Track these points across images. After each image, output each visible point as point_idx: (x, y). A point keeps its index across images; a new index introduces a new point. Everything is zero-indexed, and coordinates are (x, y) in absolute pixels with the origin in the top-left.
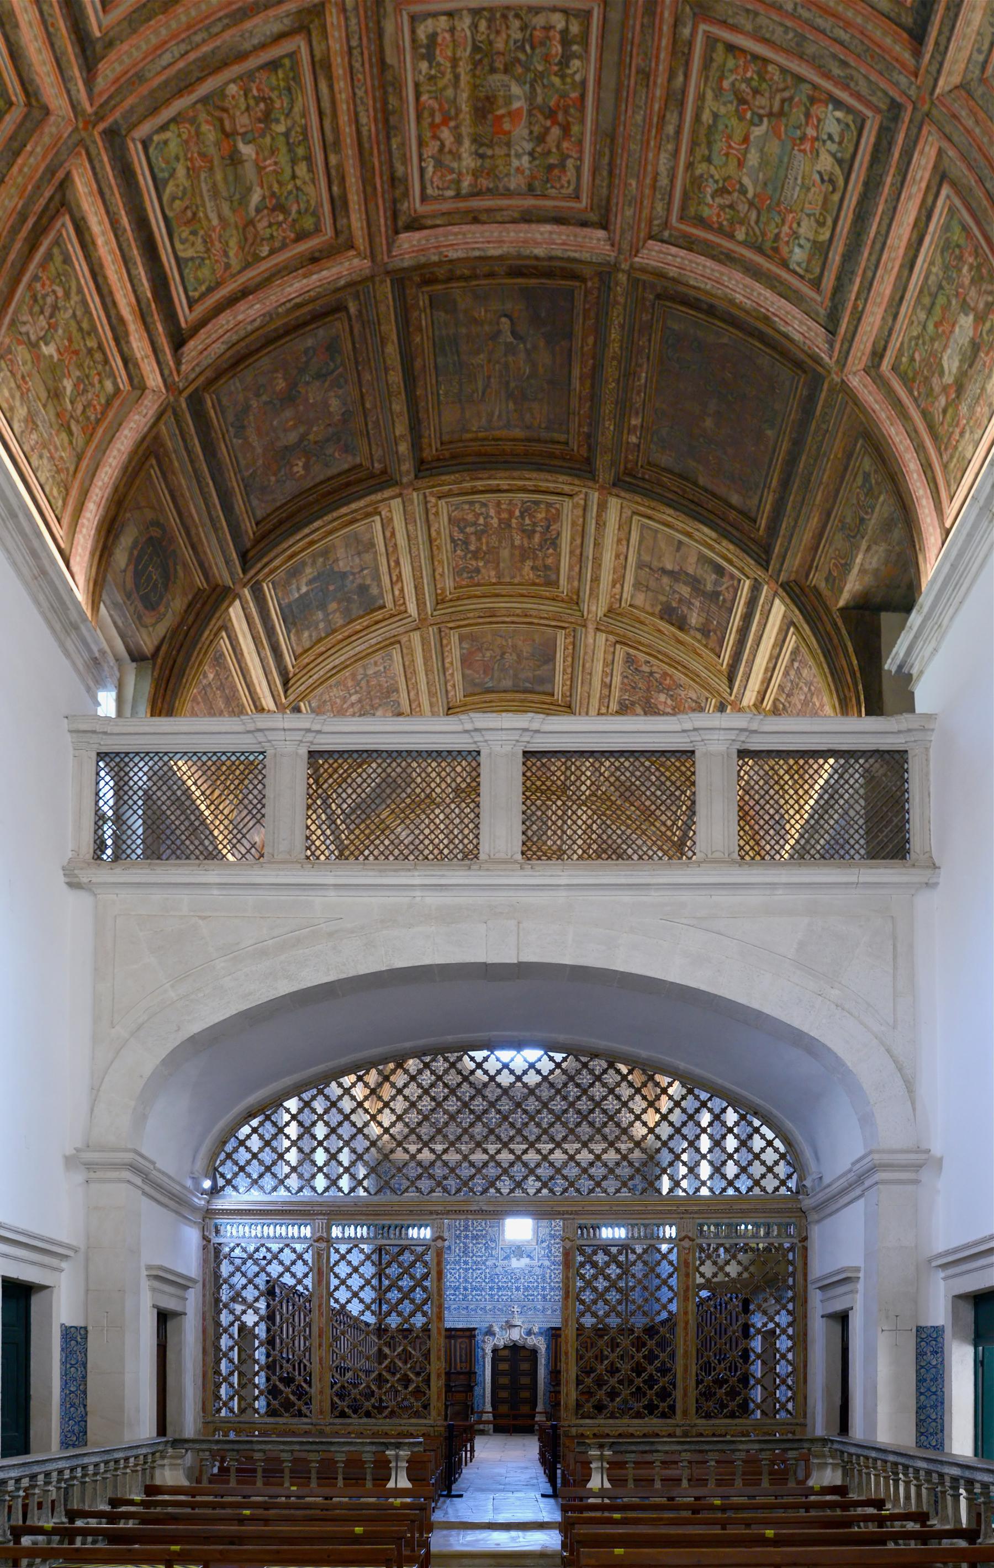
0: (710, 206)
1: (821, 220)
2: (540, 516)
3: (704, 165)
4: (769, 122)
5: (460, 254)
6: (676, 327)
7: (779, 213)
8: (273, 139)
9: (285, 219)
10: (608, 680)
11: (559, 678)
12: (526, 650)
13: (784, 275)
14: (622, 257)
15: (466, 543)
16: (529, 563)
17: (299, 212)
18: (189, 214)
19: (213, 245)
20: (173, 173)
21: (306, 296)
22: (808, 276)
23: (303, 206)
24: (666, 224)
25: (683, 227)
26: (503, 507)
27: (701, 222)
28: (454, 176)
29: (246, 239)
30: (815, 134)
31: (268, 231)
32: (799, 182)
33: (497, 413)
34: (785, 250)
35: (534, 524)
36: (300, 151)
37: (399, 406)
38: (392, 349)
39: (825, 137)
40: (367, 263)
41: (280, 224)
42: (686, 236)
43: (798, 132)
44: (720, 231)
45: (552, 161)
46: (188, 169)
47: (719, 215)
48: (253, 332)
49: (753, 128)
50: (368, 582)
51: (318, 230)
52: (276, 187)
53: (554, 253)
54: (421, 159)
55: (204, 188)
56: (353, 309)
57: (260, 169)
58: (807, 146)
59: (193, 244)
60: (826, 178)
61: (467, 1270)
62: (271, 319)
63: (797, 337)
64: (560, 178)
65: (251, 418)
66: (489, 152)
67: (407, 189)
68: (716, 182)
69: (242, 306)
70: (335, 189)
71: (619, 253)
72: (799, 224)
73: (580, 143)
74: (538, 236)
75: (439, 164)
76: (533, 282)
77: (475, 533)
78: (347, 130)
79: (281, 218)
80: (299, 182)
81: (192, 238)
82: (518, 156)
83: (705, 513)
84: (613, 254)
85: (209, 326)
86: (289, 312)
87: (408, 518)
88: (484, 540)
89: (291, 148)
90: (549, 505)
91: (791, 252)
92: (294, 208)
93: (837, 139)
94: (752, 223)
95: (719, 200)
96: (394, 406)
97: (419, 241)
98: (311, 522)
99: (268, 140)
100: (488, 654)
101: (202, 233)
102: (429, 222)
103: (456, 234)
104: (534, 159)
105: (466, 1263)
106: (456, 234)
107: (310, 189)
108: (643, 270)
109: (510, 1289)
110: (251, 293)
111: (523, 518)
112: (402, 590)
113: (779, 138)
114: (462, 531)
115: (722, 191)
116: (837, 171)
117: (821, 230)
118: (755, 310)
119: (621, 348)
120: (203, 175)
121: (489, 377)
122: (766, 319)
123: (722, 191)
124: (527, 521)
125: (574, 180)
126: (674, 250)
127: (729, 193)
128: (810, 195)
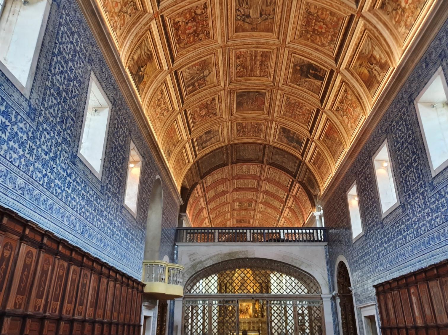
10: (220, 104)
11: (235, 99)
12: (245, 105)
16: (244, 126)
50: (282, 133)
90: (240, 136)
100: (256, 104)
112: (275, 126)
114: (259, 132)
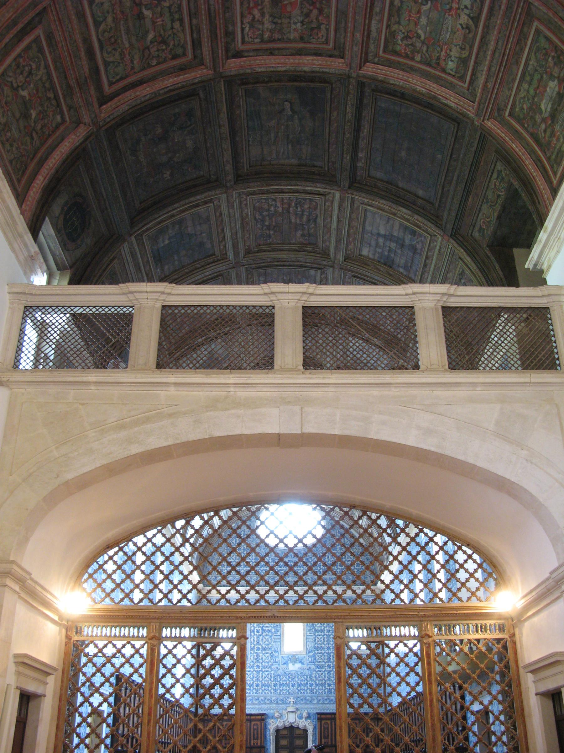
0: (400, 45)
1: (463, 47)
2: (306, 206)
3: (396, 26)
4: (432, 2)
5: (263, 70)
6: (383, 105)
7: (439, 46)
8: (162, 9)
9: (166, 49)
13: (443, 75)
14: (352, 71)
15: (263, 220)
17: (174, 45)
18: (113, 40)
19: (125, 57)
20: (105, 19)
21: (176, 86)
22: (457, 75)
23: (177, 43)
24: (376, 55)
25: (385, 56)
26: (285, 201)
27: (396, 53)
28: (260, 32)
29: (144, 56)
30: (457, 6)
31: (157, 53)
32: (450, 30)
33: (282, 150)
34: (443, 63)
35: (303, 211)
36: (177, 16)
37: (227, 145)
38: (224, 116)
39: (463, 7)
40: (211, 72)
41: (163, 50)
42: (389, 60)
43: (448, 6)
44: (406, 57)
45: (313, 26)
46: (114, 18)
47: (405, 50)
48: (145, 101)
49: (422, 6)
51: (184, 54)
52: (162, 32)
53: (314, 70)
54: (242, 23)
55: (122, 29)
56: (202, 95)
57: (154, 23)
58: (453, 12)
59: (114, 55)
60: (464, 26)
61: (258, 672)
62: (156, 96)
63: (453, 105)
64: (317, 34)
65: (141, 146)
66: (279, 21)
67: (234, 38)
68: (404, 33)
69: (139, 88)
70: (195, 35)
71: (350, 68)
72: (450, 50)
73: (328, 17)
74: (305, 61)
75: (252, 26)
76: (303, 84)
77: (269, 215)
78: (203, 7)
79: (164, 47)
80: (175, 31)
81: (114, 52)
82: (295, 23)
83: (403, 201)
84: (348, 69)
85: (120, 97)
86: (166, 93)
87: (230, 206)
88: (274, 220)
89: (171, 13)
91: (447, 64)
92: (172, 43)
93: (469, 7)
94: (424, 52)
95: (404, 42)
96: (223, 145)
97: (240, 63)
98: (173, 204)
99: (159, 9)
101: (119, 50)
102: (246, 54)
103: (260, 60)
104: (303, 25)
105: (258, 667)
106: (260, 60)
107: (181, 35)
108: (364, 77)
109: (288, 685)
110: (145, 83)
111: (297, 208)
113: (437, 10)
115: (407, 37)
116: (471, 23)
117: (463, 52)
118: (428, 93)
119: (352, 116)
120: (122, 22)
121: (278, 132)
122: (435, 98)
123: (407, 37)
124: (299, 209)
125: (325, 35)
126: (381, 67)
127: (411, 38)
128: (456, 36)
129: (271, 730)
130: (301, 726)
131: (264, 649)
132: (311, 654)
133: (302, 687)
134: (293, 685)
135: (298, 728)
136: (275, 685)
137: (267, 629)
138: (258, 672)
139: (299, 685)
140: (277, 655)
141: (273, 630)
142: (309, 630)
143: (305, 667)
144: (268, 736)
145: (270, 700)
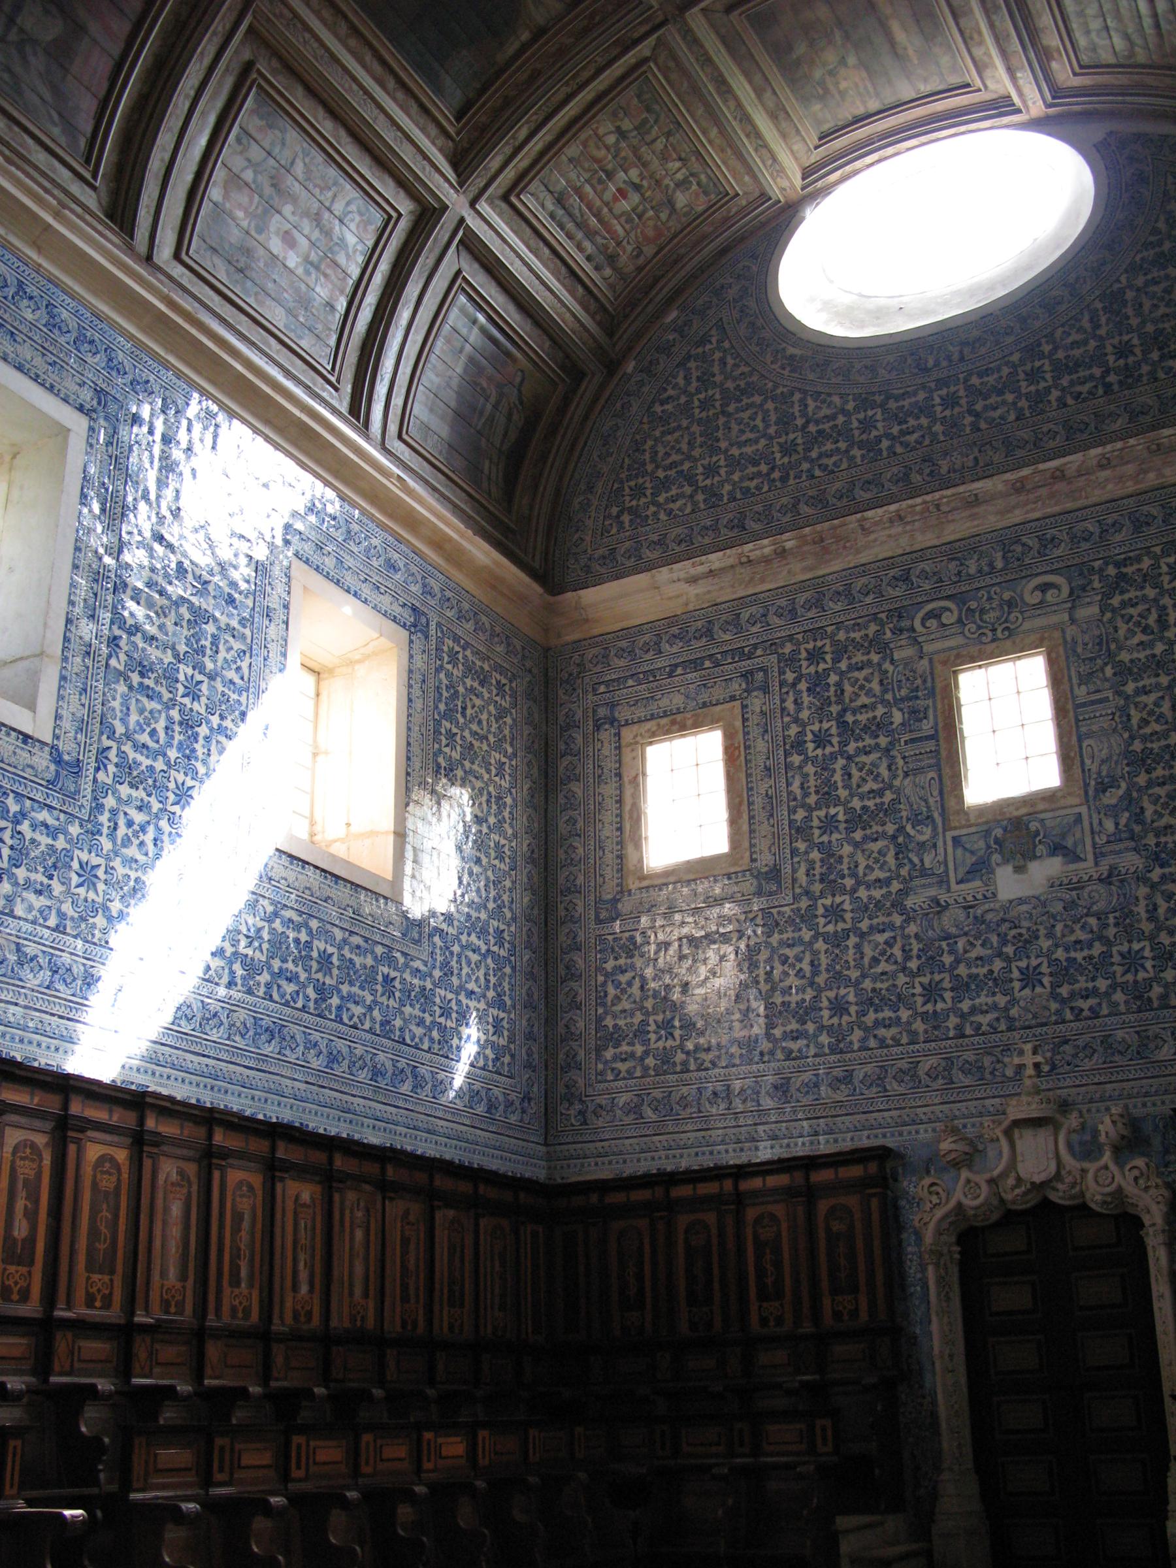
105: (835, 913)
109: (1000, 983)
129: (929, 1237)
130: (1096, 1193)
131: (856, 820)
132: (1111, 798)
133: (1082, 983)
134: (1030, 978)
135: (1083, 1209)
136: (932, 992)
137: (863, 718)
138: (837, 941)
139: (1063, 973)
140: (926, 834)
141: (898, 717)
142: (1084, 680)
143: (1087, 867)
144: (912, 1270)
145: (910, 1074)
